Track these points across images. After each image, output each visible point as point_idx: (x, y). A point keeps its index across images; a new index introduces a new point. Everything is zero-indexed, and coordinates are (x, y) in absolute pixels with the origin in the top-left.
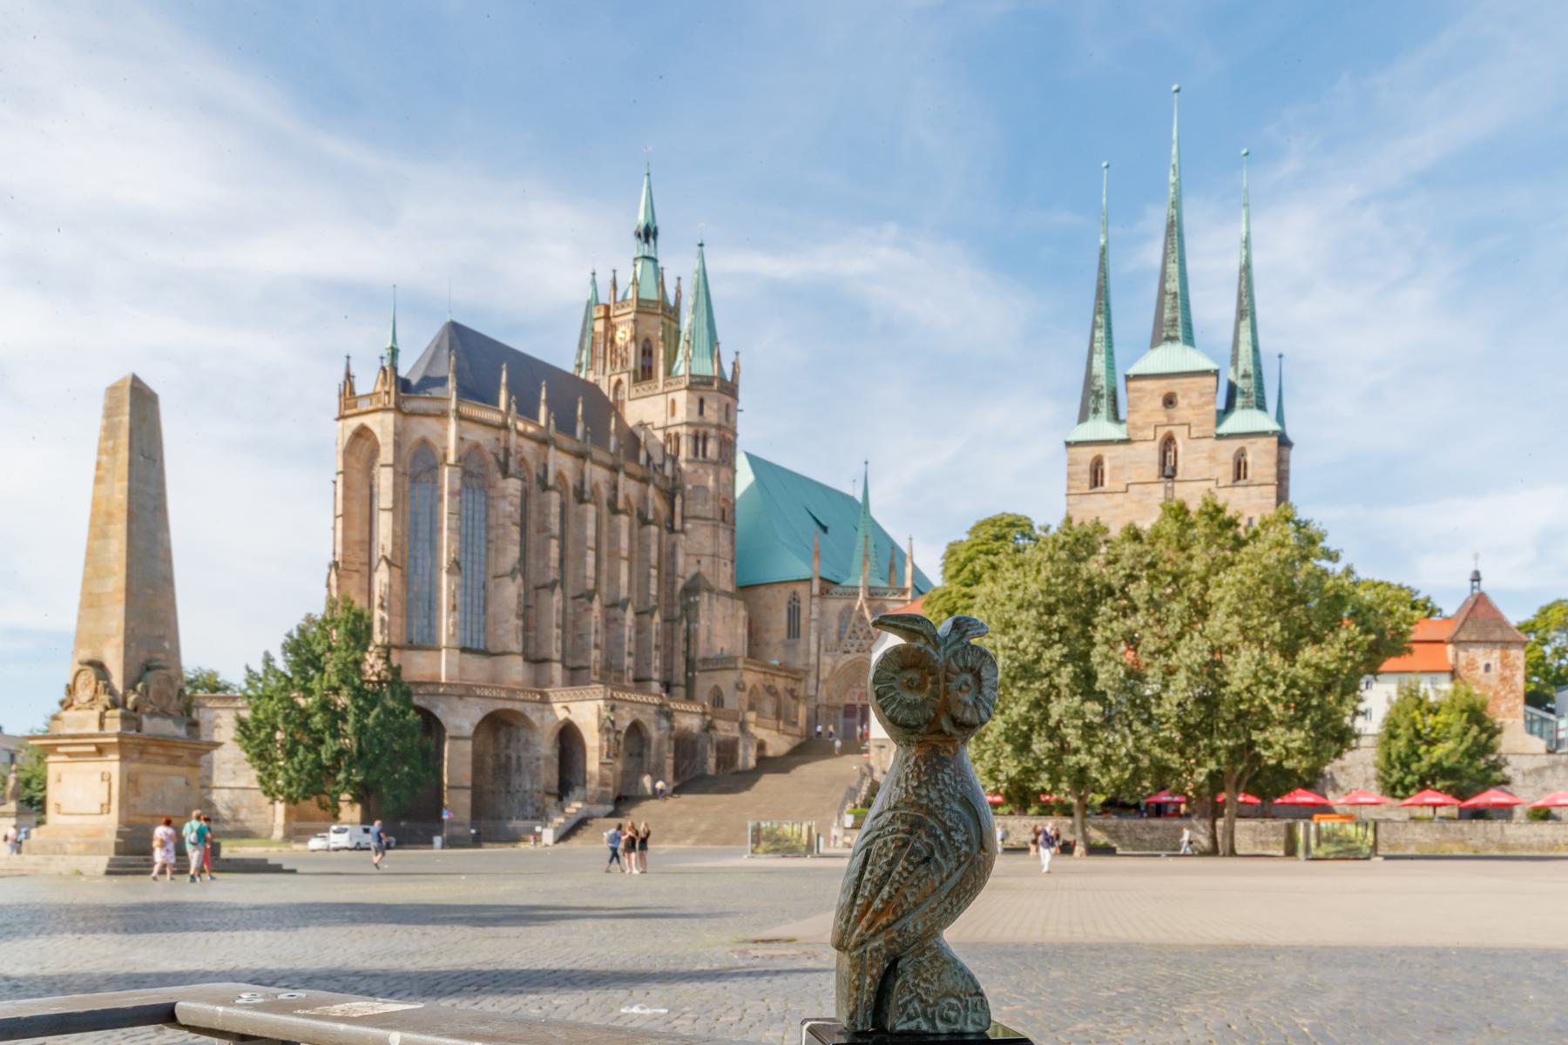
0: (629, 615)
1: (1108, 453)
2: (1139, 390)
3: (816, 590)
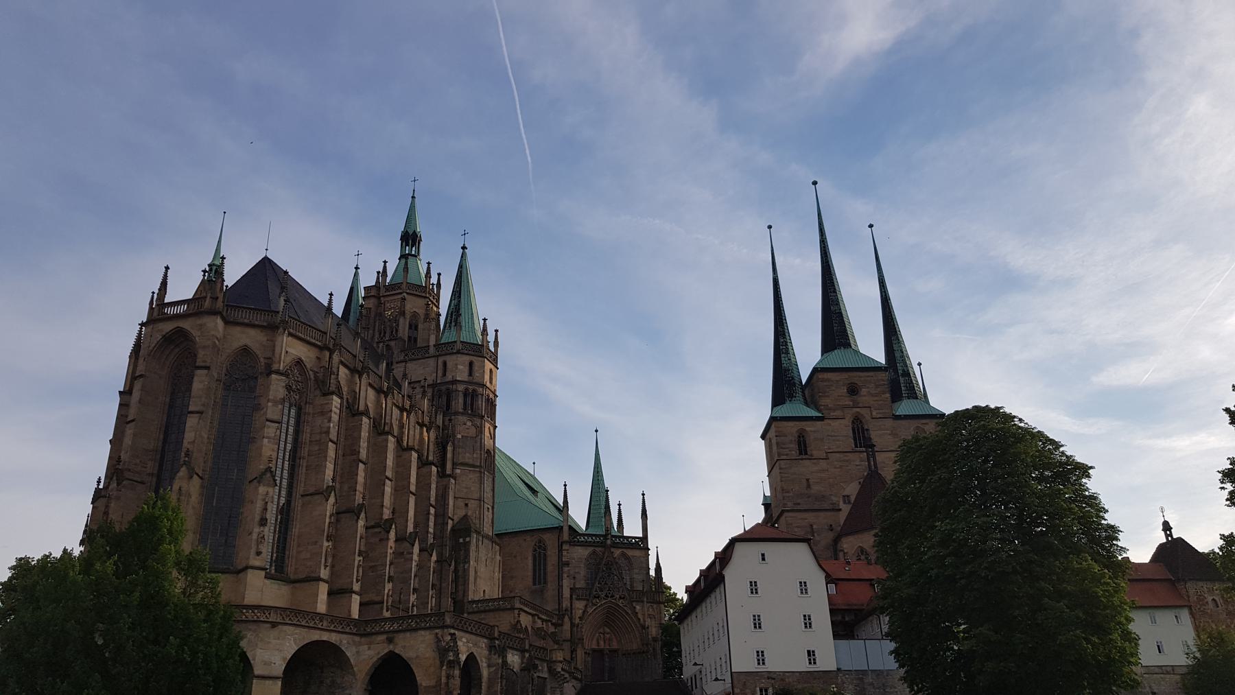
2: (828, 380)
3: (566, 536)
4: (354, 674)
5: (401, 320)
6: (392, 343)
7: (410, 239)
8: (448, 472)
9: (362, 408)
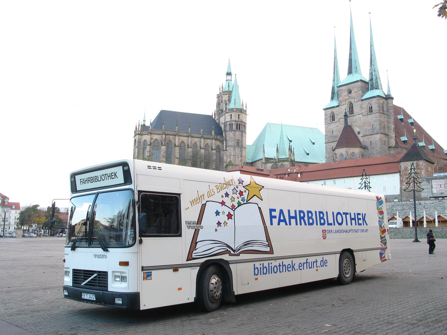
1: (334, 110)
2: (342, 90)
8: (225, 149)
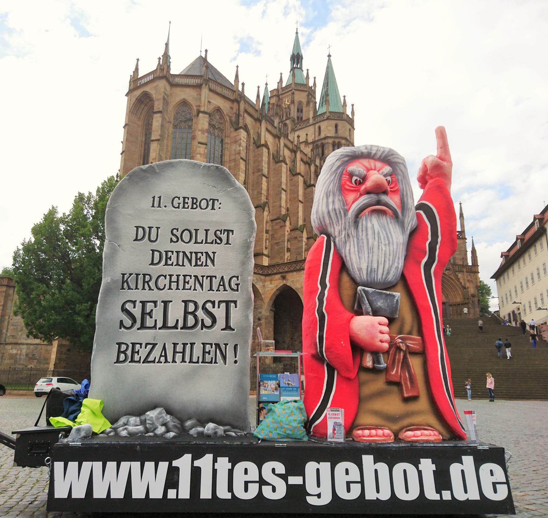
0: (305, 235)
4: (262, 300)
5: (292, 107)
6: (288, 122)
7: (297, 59)
9: (263, 142)
